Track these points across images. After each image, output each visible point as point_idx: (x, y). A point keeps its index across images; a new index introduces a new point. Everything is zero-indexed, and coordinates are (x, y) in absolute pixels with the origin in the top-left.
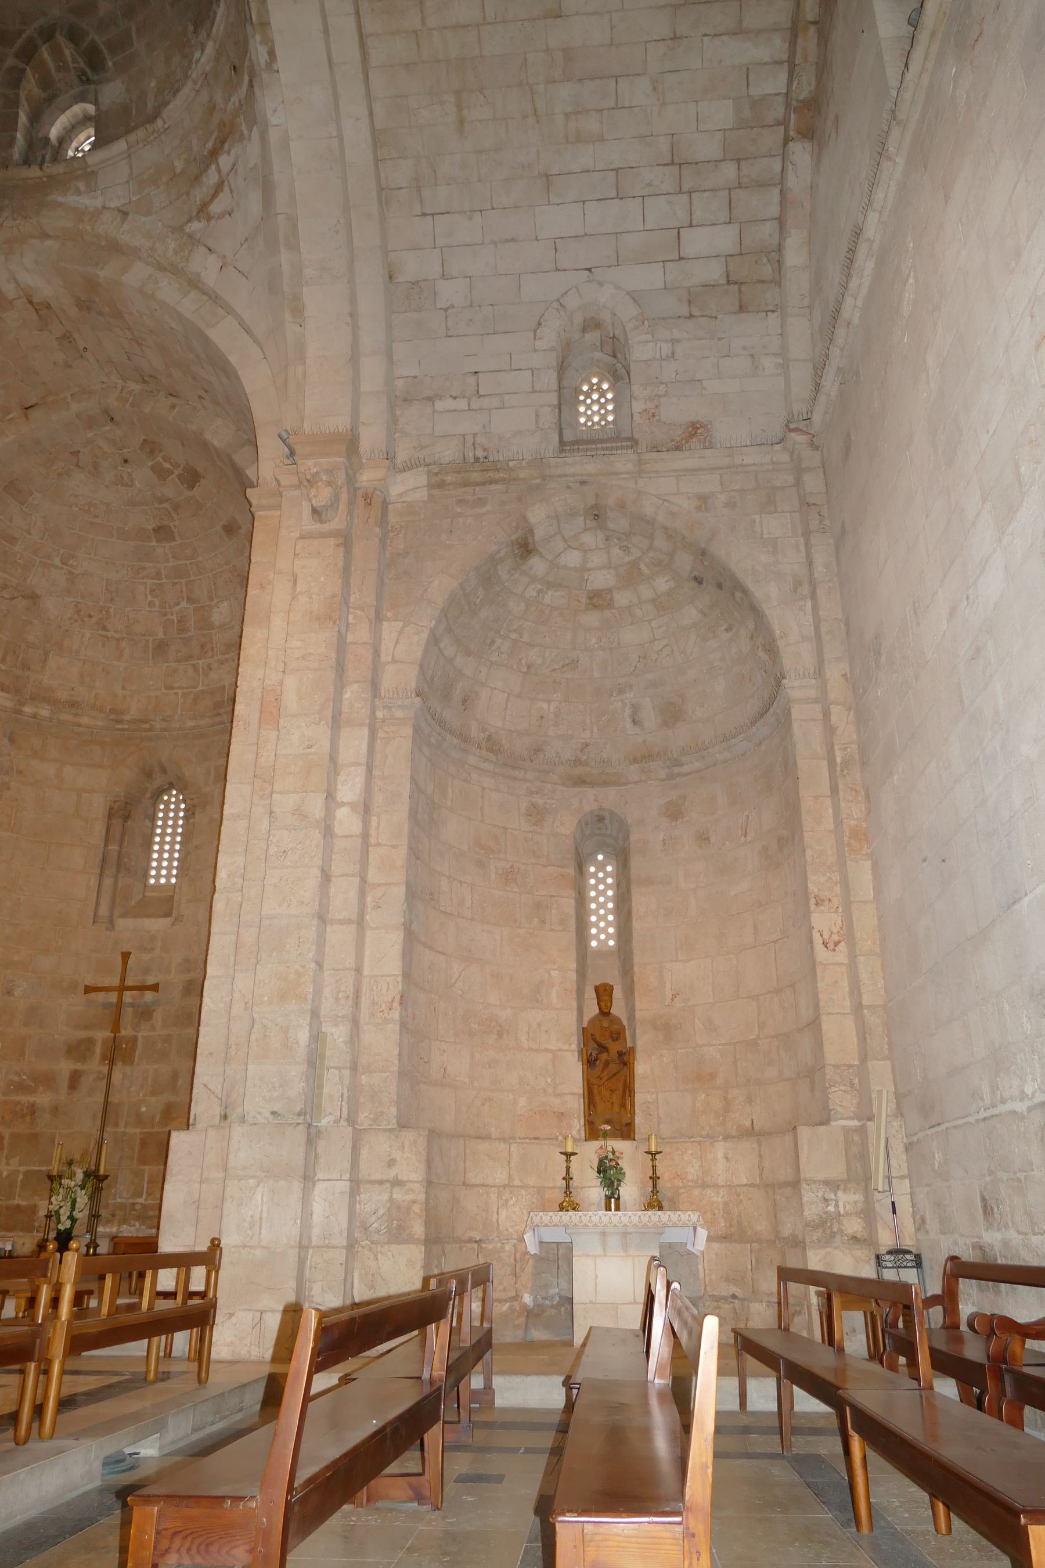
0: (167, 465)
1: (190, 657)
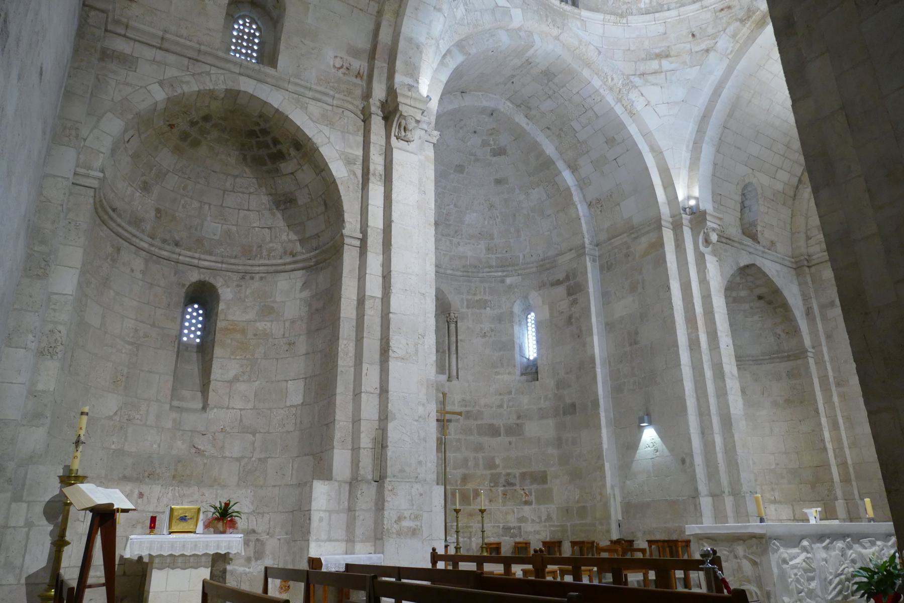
0: (492, 142)
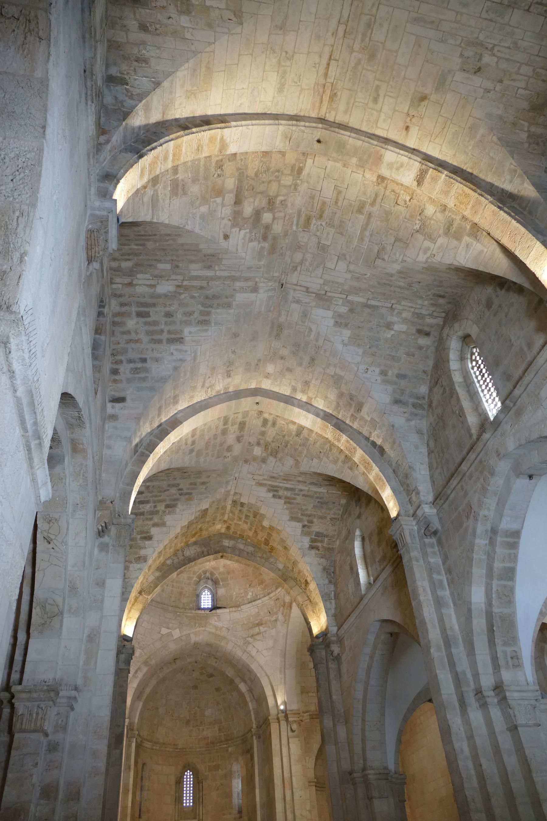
1: (197, 726)
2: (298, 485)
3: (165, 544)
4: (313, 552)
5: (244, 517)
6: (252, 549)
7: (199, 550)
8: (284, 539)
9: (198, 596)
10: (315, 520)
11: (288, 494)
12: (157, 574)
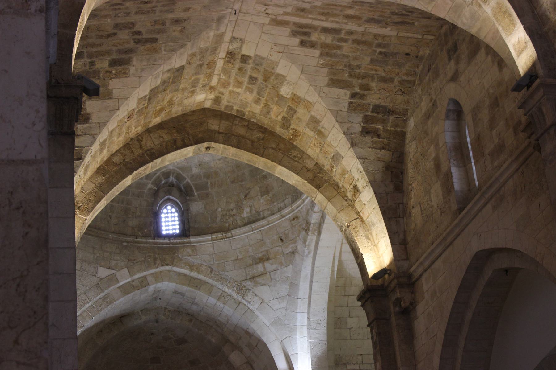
2: (346, 23)
3: (111, 129)
4: (368, 139)
5: (246, 80)
6: (261, 135)
7: (167, 137)
8: (318, 117)
9: (156, 215)
10: (373, 84)
11: (328, 39)
12: (100, 179)
